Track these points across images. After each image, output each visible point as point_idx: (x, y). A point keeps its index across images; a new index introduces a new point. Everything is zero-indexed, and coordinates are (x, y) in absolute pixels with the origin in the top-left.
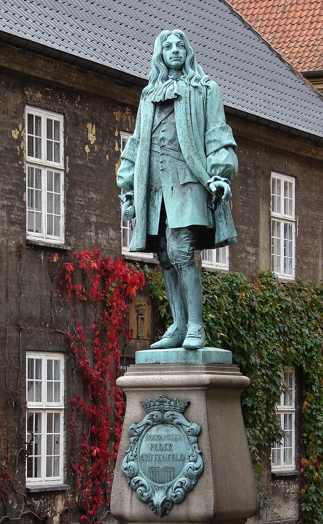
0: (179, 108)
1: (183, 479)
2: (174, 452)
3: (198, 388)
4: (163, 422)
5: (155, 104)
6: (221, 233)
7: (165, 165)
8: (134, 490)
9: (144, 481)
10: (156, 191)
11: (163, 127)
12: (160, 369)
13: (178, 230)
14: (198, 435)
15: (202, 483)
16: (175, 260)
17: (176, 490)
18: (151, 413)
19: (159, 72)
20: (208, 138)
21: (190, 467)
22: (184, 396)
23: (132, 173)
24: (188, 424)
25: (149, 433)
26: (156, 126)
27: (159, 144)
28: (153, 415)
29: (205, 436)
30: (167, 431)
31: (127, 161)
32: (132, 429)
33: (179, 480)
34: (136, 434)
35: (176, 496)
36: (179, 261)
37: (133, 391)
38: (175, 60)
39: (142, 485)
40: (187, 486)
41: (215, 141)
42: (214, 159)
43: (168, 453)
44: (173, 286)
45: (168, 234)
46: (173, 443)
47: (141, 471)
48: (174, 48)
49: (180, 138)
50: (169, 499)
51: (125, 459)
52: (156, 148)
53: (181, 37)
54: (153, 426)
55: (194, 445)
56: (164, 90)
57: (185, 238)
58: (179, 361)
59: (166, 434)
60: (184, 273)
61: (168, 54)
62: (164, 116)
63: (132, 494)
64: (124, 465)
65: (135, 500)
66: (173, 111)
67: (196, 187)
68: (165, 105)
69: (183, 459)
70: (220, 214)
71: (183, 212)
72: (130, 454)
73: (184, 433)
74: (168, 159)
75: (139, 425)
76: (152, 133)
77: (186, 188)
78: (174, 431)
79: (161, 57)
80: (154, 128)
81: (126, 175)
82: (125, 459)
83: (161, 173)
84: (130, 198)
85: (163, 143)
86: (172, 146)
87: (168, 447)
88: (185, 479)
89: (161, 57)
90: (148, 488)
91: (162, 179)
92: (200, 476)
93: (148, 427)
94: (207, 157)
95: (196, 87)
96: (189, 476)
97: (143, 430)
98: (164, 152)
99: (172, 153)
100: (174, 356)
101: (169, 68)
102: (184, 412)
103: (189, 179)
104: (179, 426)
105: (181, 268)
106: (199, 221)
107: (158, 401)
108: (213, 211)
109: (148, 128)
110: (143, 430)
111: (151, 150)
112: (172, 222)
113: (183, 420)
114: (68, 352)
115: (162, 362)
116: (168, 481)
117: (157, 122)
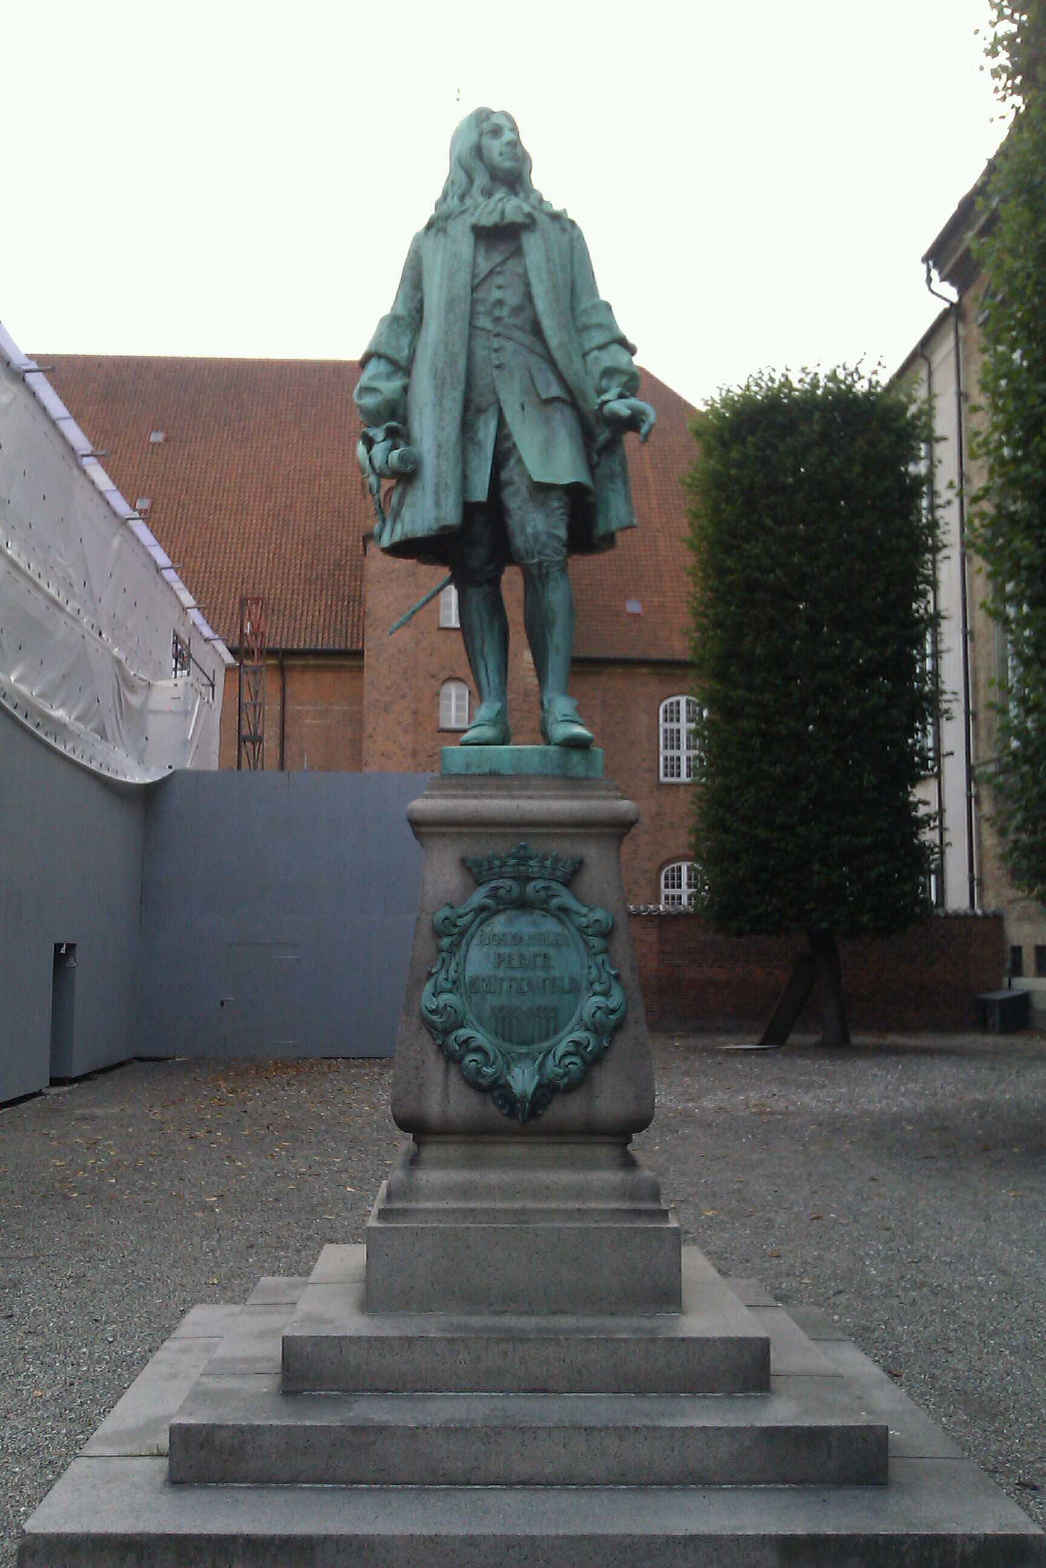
0: (531, 243)
1: (579, 1035)
2: (556, 973)
3: (605, 830)
4: (523, 905)
6: (613, 514)
7: (507, 357)
8: (452, 1059)
9: (482, 1038)
10: (480, 411)
11: (499, 280)
12: (509, 788)
13: (541, 490)
14: (607, 934)
16: (540, 553)
17: (567, 1061)
18: (493, 884)
21: (599, 1008)
22: (564, 848)
23: (397, 383)
24: (584, 910)
25: (487, 929)
26: (482, 275)
27: (489, 313)
28: (497, 888)
30: (535, 924)
31: (383, 361)
32: (446, 918)
33: (571, 1038)
34: (456, 930)
35: (565, 1074)
36: (547, 555)
37: (443, 835)
38: (509, 159)
39: (479, 1049)
40: (591, 1052)
43: (541, 974)
44: (486, 625)
45: (516, 501)
46: (552, 952)
47: (470, 1016)
49: (542, 304)
50: (545, 1081)
51: (429, 987)
54: (497, 912)
55: (600, 958)
56: (500, 205)
57: (558, 508)
58: (546, 771)
59: (532, 930)
60: (552, 584)
62: (497, 258)
63: (447, 1070)
66: (518, 252)
67: (568, 412)
69: (575, 989)
70: (612, 476)
71: (550, 456)
72: (442, 975)
73: (573, 930)
74: (510, 346)
75: (462, 912)
76: (474, 289)
78: (550, 926)
80: (477, 281)
81: (390, 387)
82: (429, 987)
83: (495, 372)
85: (497, 313)
86: (518, 321)
87: (539, 961)
88: (586, 1034)
90: (492, 1057)
91: (500, 387)
92: (619, 1026)
93: (484, 915)
94: (585, 355)
96: (596, 1029)
97: (473, 922)
98: (499, 329)
99: (517, 334)
100: (536, 759)
103: (555, 391)
104: (562, 915)
105: (548, 574)
106: (583, 478)
107: (515, 857)
109: (463, 278)
110: (473, 922)
111: (472, 326)
116: (540, 1040)
117: (484, 267)
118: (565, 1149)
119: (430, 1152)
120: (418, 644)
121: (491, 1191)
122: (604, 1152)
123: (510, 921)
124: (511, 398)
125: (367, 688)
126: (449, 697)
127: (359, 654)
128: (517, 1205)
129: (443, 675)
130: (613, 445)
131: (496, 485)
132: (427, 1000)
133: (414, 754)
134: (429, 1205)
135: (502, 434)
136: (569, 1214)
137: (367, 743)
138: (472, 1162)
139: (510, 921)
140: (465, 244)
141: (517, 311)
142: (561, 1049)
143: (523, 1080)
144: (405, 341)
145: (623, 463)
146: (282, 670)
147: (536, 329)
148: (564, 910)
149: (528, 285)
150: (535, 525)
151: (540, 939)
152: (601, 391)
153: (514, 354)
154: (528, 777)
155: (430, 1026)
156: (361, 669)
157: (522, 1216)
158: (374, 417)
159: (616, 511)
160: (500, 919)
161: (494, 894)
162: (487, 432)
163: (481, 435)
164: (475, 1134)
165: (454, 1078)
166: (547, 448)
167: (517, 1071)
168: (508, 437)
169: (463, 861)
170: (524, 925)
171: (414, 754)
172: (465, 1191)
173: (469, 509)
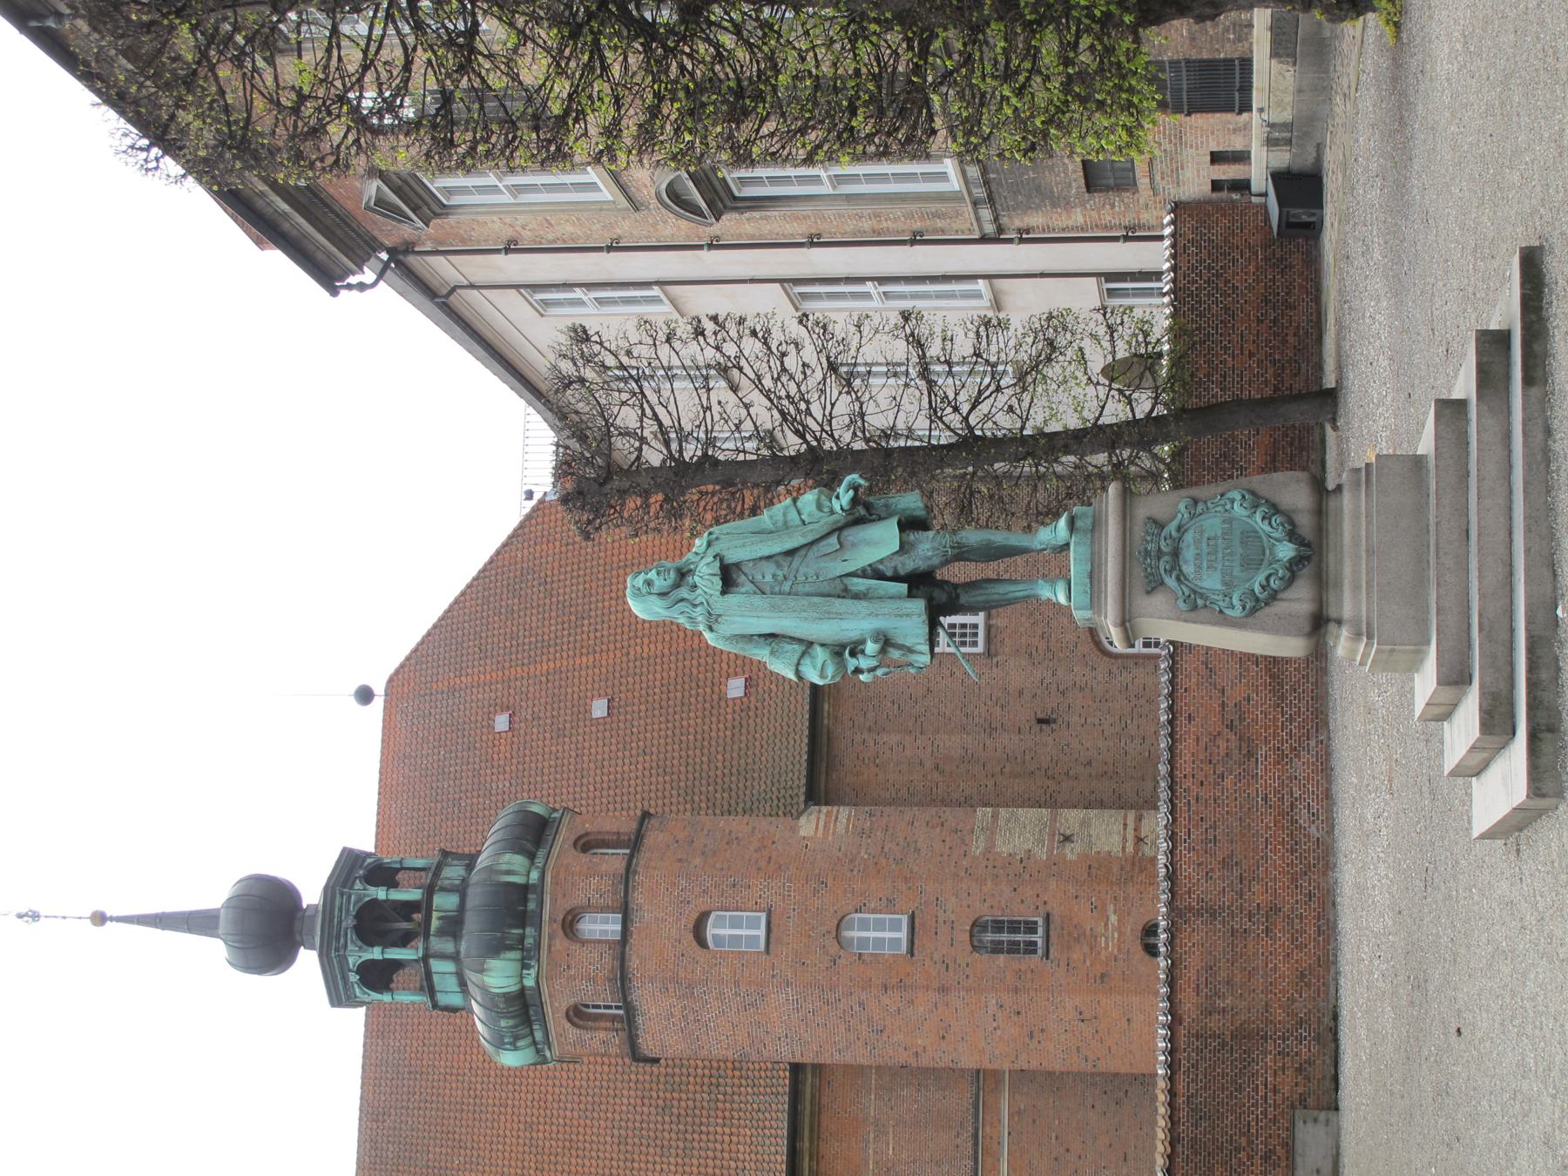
0: (732, 557)
1: (1258, 517)
2: (1219, 533)
4: (1176, 554)
5: (724, 593)
6: (912, 505)
7: (811, 572)
8: (1274, 596)
9: (1261, 578)
10: (846, 590)
12: (1100, 565)
13: (904, 548)
14: (1196, 502)
15: (1264, 490)
19: (682, 600)
23: (818, 650)
27: (781, 584)
39: (1268, 578)
41: (785, 515)
45: (909, 564)
48: (652, 575)
61: (660, 583)
62: (743, 577)
66: (737, 565)
67: (846, 533)
68: (728, 576)
69: (1229, 521)
74: (803, 570)
77: (846, 543)
78: (1189, 537)
79: (662, 595)
81: (820, 654)
82: (1228, 612)
85: (781, 578)
89: (662, 595)
96: (1255, 507)
101: (677, 586)
102: (1161, 525)
106: (894, 521)
108: (880, 519)
109: (757, 600)
113: (1174, 524)
115: (1088, 568)
117: (749, 587)
118: (1331, 528)
119: (1333, 613)
121: (1356, 572)
122: (1332, 503)
123: (1186, 562)
124: (840, 568)
125: (848, 1058)
126: (863, 942)
127: (796, 1069)
128: (1364, 555)
129: (834, 948)
131: (896, 578)
132: (1237, 612)
133: (943, 990)
134: (1364, 609)
135: (863, 574)
136: (1369, 523)
137: (925, 1061)
138: (1339, 585)
139: (1186, 562)
140: (732, 599)
141: (779, 566)
142: (1267, 528)
143: (1286, 551)
144: (788, 647)
147: (791, 553)
148: (1179, 528)
149: (761, 558)
151: (1197, 542)
152: (832, 512)
153: (807, 567)
154: (1092, 554)
155: (1254, 610)
156: (818, 1068)
157: (1370, 552)
158: (841, 664)
160: (1184, 568)
161: (1169, 572)
162: (860, 584)
163: (862, 588)
164: (1322, 583)
165: (1286, 595)
167: (1281, 555)
168: (864, 570)
169: (1148, 593)
170: (1188, 553)
171: (943, 990)
172: (1356, 588)
173: (910, 595)
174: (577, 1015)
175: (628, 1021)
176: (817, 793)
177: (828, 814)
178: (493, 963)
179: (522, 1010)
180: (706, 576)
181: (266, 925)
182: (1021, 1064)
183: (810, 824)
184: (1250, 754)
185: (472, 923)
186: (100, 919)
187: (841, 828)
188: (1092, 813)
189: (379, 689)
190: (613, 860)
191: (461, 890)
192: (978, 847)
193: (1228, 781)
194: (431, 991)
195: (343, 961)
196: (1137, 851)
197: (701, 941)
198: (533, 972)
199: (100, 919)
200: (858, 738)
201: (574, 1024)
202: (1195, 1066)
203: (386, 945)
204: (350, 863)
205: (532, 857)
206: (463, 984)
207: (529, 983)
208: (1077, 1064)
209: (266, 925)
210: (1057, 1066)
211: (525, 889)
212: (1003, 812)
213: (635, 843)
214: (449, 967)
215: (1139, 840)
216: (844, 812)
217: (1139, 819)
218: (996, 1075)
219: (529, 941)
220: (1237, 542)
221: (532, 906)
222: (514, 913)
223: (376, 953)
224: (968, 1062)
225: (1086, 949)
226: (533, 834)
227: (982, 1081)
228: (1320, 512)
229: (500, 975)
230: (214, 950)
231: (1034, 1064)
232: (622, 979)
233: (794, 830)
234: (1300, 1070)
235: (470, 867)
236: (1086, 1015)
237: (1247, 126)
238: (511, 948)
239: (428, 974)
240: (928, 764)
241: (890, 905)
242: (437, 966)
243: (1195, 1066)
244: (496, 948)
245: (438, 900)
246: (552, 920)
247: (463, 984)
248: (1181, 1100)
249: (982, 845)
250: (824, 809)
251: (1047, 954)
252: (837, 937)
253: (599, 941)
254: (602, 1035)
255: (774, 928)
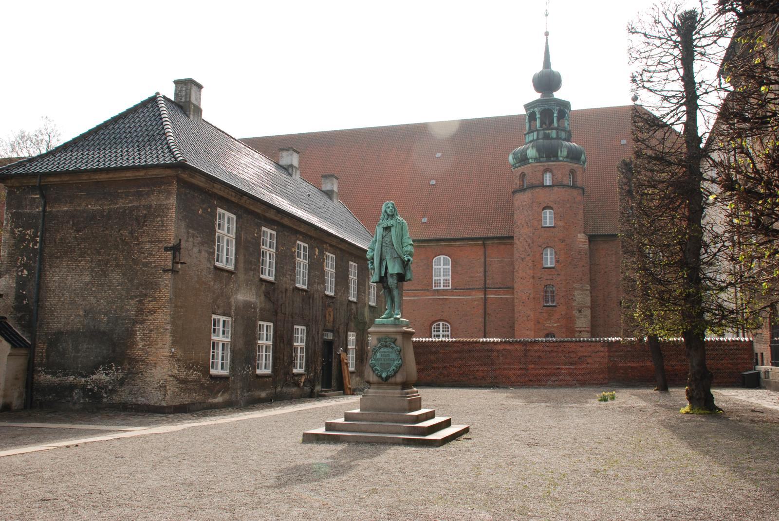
1: (394, 368)
4: (386, 346)
5: (384, 228)
8: (374, 372)
9: (378, 368)
13: (392, 275)
20: (403, 241)
22: (393, 336)
29: (402, 351)
42: (405, 249)
48: (391, 208)
49: (393, 241)
52: (384, 244)
53: (393, 204)
61: (388, 210)
64: (370, 362)
65: (374, 375)
66: (390, 231)
68: (387, 229)
69: (394, 360)
71: (394, 268)
78: (390, 350)
79: (386, 211)
81: (371, 254)
84: (372, 263)
89: (386, 211)
92: (401, 366)
95: (399, 223)
96: (396, 367)
101: (388, 215)
103: (396, 256)
106: (400, 272)
109: (381, 237)
111: (382, 245)
112: (390, 271)
113: (394, 346)
114: (307, 326)
117: (384, 234)
119: (372, 386)
120: (533, 234)
124: (388, 257)
125: (515, 252)
126: (547, 254)
127: (512, 238)
129: (544, 246)
130: (407, 264)
133: (533, 278)
137: (515, 274)
138: (378, 388)
141: (390, 242)
145: (410, 267)
146: (484, 245)
147: (393, 245)
148: (393, 347)
150: (392, 282)
156: (512, 244)
157: (384, 397)
159: (408, 276)
164: (379, 383)
166: (394, 267)
170: (386, 350)
171: (533, 278)
172: (376, 393)
174: (523, 175)
175: (522, 190)
176: (592, 238)
177: (586, 242)
178: (535, 150)
179: (523, 159)
180: (390, 222)
181: (547, 82)
182: (516, 300)
183: (581, 237)
184: (571, 364)
185: (547, 142)
186: (547, 34)
187: (581, 246)
188: (589, 318)
189: (638, 102)
190: (567, 181)
191: (558, 138)
192: (576, 285)
193: (563, 358)
194: (529, 133)
195: (536, 107)
196: (577, 331)
197: (544, 208)
198: (533, 161)
199: (547, 34)
200: (614, 249)
201: (520, 175)
202: (483, 349)
203: (540, 118)
204: (566, 105)
205: (567, 157)
206: (530, 142)
207: (530, 161)
208: (516, 315)
209: (547, 82)
210: (516, 310)
211: (556, 156)
212: (588, 293)
213: (574, 187)
214: (535, 137)
215: (580, 332)
216: (586, 246)
217: (588, 332)
218: (513, 293)
219: (542, 159)
220: (388, 362)
221: (552, 159)
222: (549, 153)
223: (538, 116)
224: (516, 286)
225: (547, 317)
226: (575, 156)
227: (511, 289)
228: (396, 384)
229: (531, 153)
230: (539, 68)
231: (516, 304)
232: (532, 187)
233: (580, 232)
234: (483, 377)
235: (565, 140)
236: (529, 318)
237: (768, 365)
238: (539, 155)
239: (533, 132)
240: (606, 270)
241: (557, 261)
242: (535, 134)
243: (483, 349)
244: (539, 150)
245: (554, 132)
246: (548, 165)
247: (530, 142)
248: (474, 345)
249: (577, 287)
250: (587, 241)
251: (545, 306)
252: (547, 247)
253: (543, 179)
254: (518, 183)
255: (549, 229)
